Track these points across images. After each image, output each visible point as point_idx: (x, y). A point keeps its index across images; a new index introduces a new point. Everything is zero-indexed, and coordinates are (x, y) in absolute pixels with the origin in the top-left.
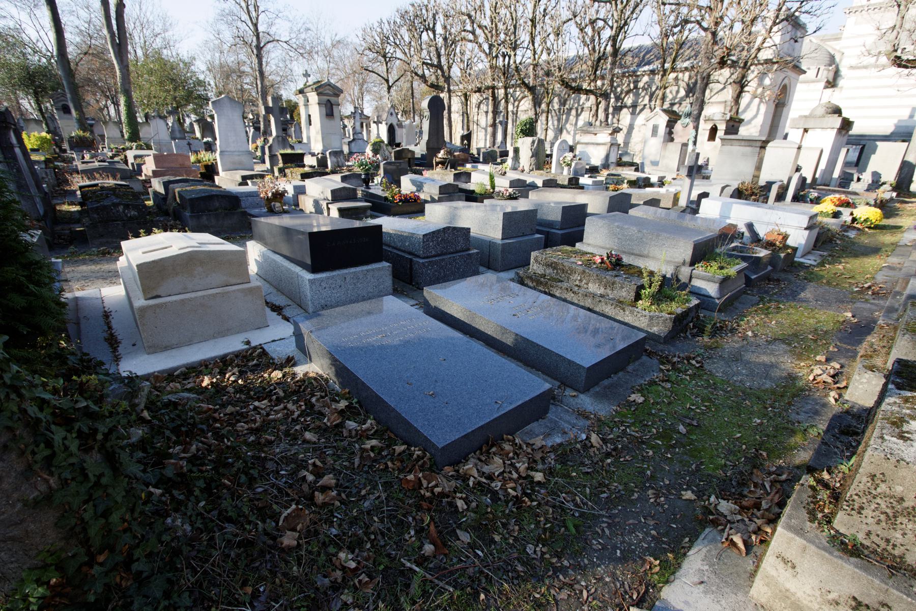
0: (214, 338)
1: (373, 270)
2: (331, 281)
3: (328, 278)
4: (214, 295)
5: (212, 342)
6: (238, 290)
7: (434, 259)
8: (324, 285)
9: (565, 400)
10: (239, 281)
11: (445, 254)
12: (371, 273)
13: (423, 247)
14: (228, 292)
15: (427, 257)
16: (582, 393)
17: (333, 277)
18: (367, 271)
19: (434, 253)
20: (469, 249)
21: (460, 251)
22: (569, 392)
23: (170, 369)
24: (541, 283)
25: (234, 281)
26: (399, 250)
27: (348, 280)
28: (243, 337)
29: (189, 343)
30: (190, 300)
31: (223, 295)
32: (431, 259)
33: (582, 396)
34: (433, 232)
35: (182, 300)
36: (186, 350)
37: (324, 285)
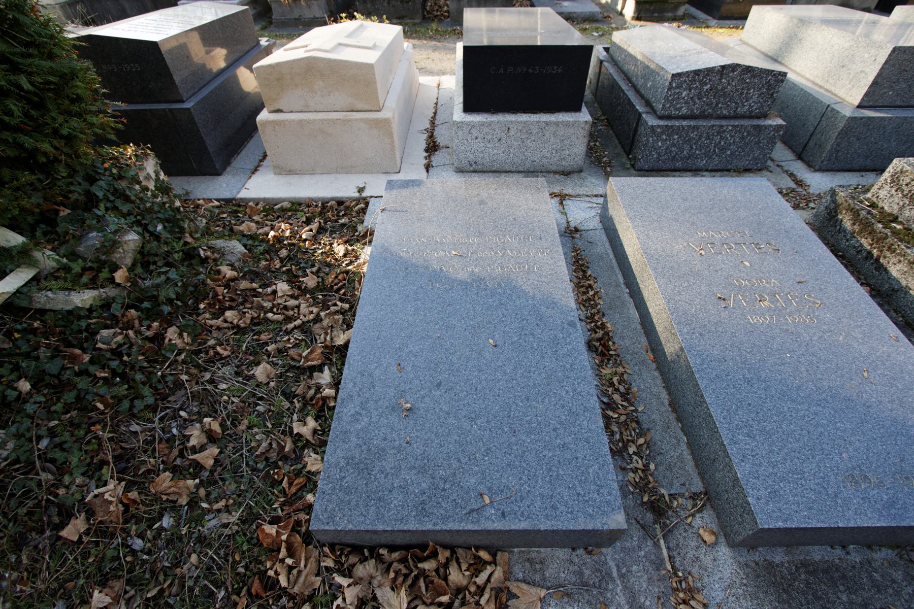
0: (338, 172)
1: (557, 124)
2: (486, 130)
3: (483, 124)
4: (334, 122)
5: (332, 177)
6: (361, 120)
7: (677, 123)
8: (475, 133)
9: (679, 534)
10: (366, 108)
11: (703, 116)
12: (552, 128)
13: (666, 99)
14: (350, 120)
15: (669, 118)
16: (732, 545)
17: (490, 124)
18: (547, 124)
19: (684, 111)
20: (765, 116)
21: (743, 117)
22: (704, 523)
23: (273, 199)
24: (872, 232)
25: (360, 106)
26: (637, 91)
27: (512, 132)
28: (359, 180)
29: (311, 171)
30: (309, 122)
31: (345, 122)
32: (669, 123)
33: (724, 551)
34: (697, 72)
35: (301, 121)
36: (307, 179)
37: (475, 133)
